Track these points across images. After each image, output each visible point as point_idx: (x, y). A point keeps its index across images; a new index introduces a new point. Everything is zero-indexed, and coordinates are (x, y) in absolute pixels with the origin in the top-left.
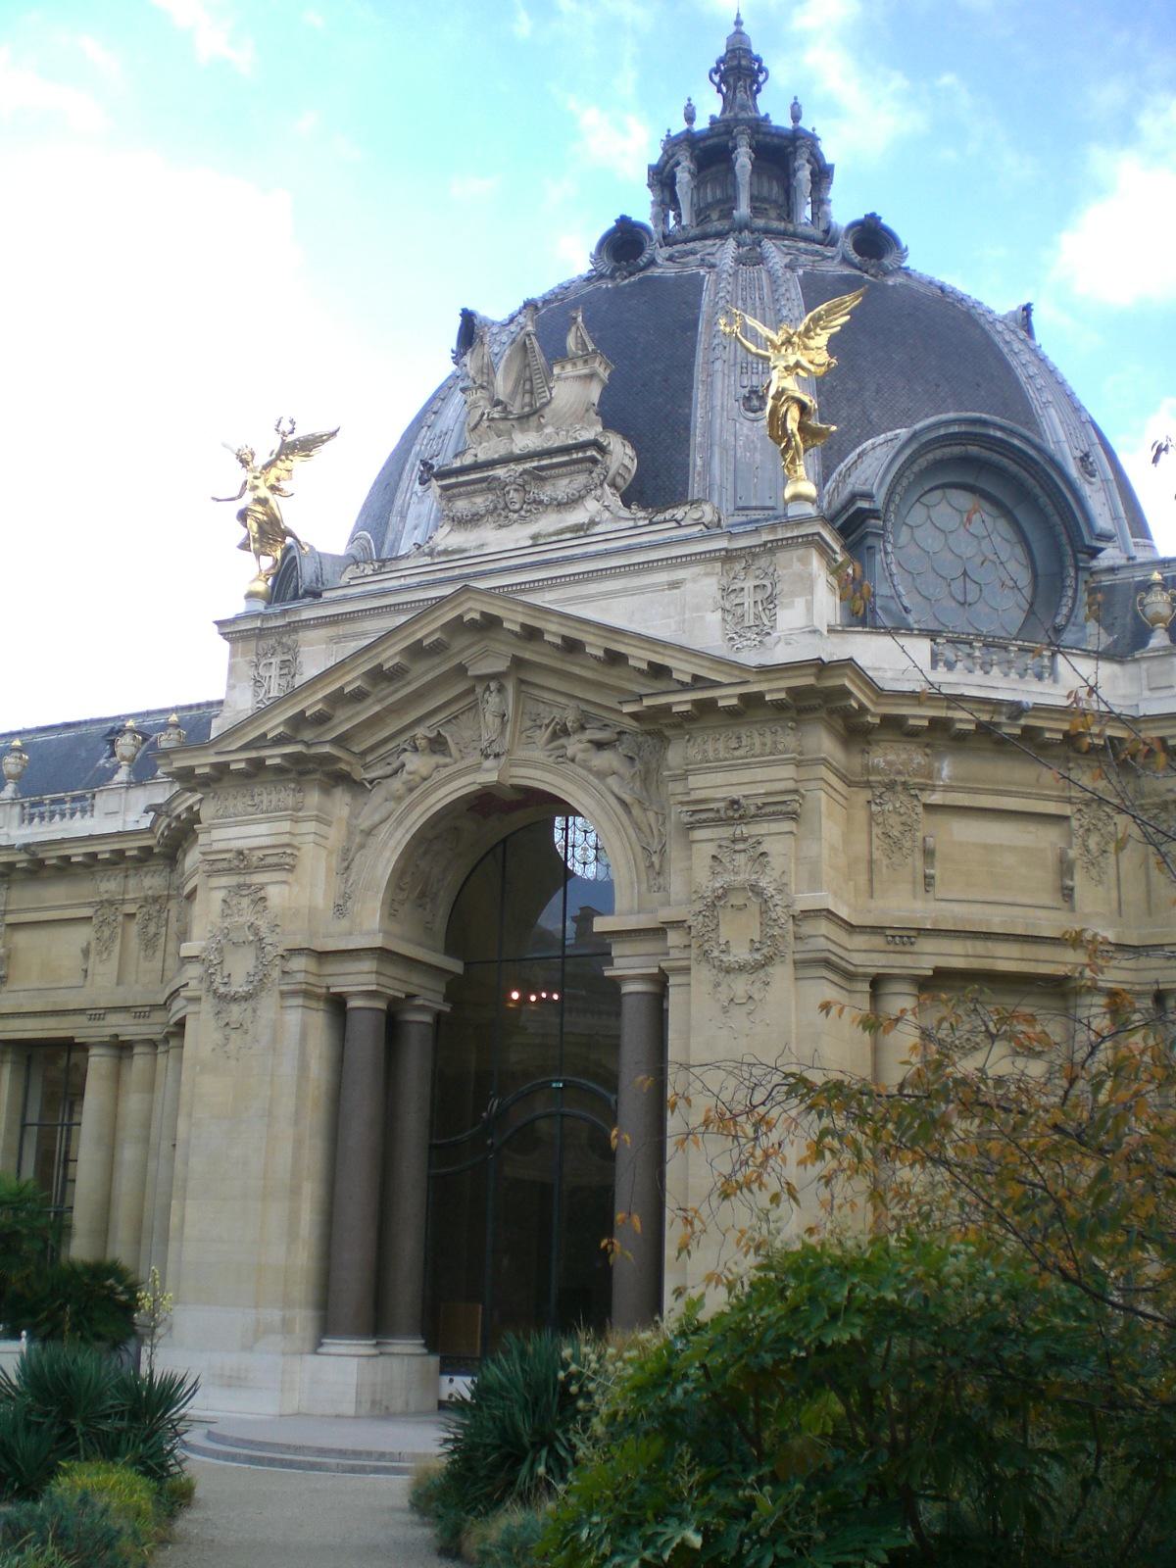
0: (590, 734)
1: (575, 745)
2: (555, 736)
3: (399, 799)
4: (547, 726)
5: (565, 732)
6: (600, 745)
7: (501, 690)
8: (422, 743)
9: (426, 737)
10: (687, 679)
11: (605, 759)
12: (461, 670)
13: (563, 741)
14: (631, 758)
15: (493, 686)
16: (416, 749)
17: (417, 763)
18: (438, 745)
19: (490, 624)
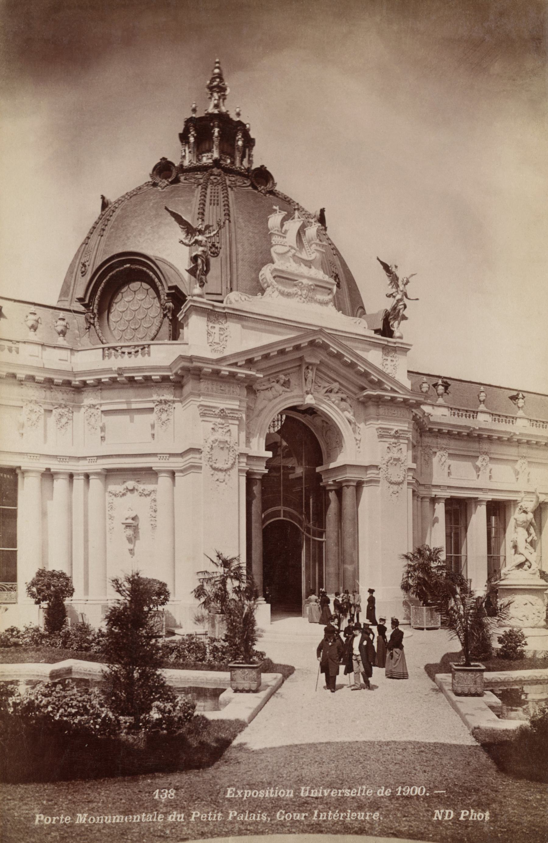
0: (341, 395)
1: (334, 397)
2: (326, 392)
3: (270, 400)
4: (324, 387)
5: (331, 391)
6: (342, 400)
7: (312, 370)
8: (282, 381)
9: (285, 380)
10: (389, 389)
11: (343, 404)
12: (301, 359)
13: (328, 394)
14: (351, 406)
15: (310, 367)
16: (278, 382)
17: (278, 387)
18: (286, 384)
19: (325, 347)
